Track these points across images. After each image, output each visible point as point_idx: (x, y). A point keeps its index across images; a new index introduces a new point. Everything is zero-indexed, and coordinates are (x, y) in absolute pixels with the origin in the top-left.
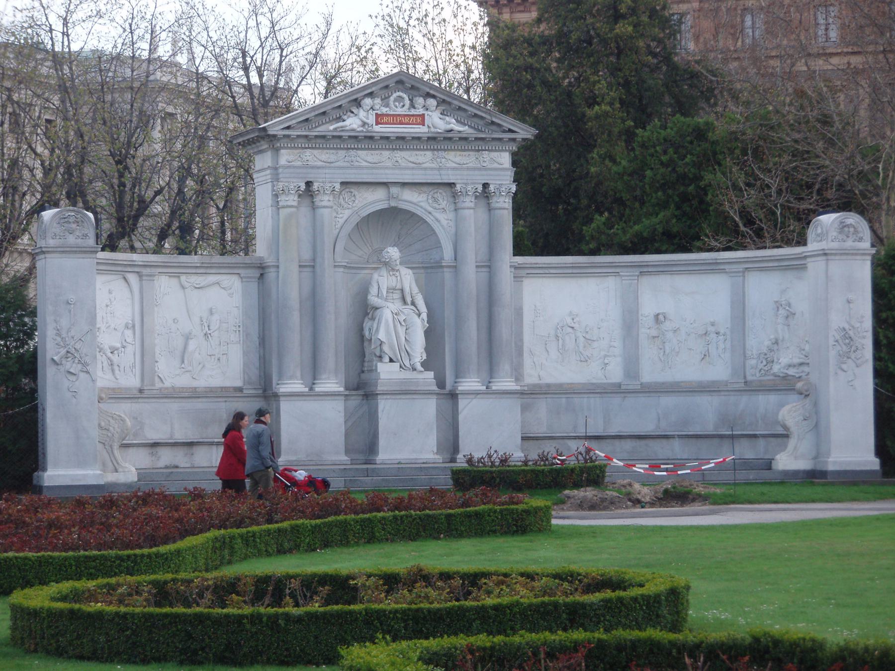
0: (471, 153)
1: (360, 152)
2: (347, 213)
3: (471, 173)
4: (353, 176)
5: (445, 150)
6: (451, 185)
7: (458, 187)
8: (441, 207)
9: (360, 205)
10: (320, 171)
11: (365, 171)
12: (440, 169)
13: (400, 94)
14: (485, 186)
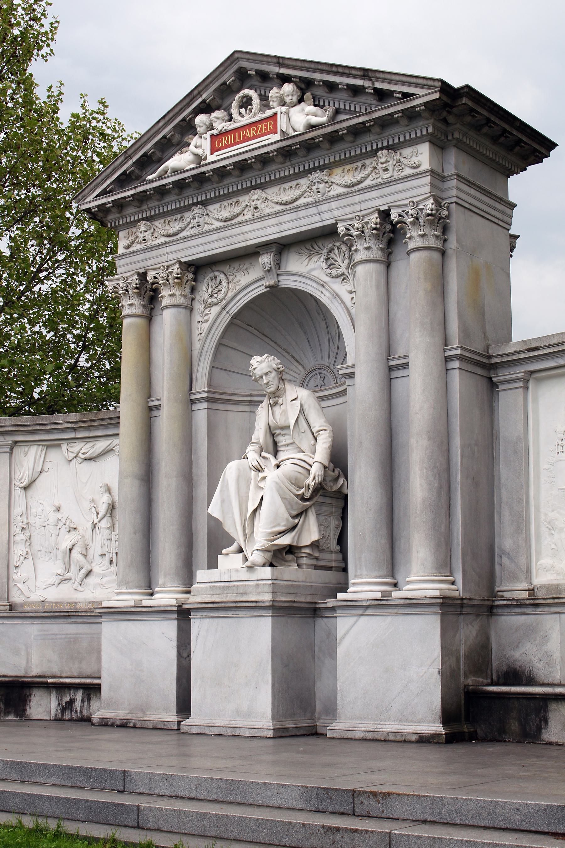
0: (367, 162)
1: (211, 208)
2: (215, 310)
3: (368, 196)
4: (200, 249)
5: (321, 168)
6: (334, 227)
7: (341, 229)
8: (339, 271)
9: (230, 295)
10: (160, 251)
11: (215, 237)
12: (316, 203)
13: (241, 94)
14: (385, 215)
